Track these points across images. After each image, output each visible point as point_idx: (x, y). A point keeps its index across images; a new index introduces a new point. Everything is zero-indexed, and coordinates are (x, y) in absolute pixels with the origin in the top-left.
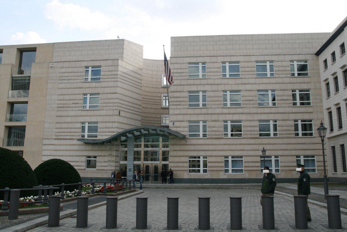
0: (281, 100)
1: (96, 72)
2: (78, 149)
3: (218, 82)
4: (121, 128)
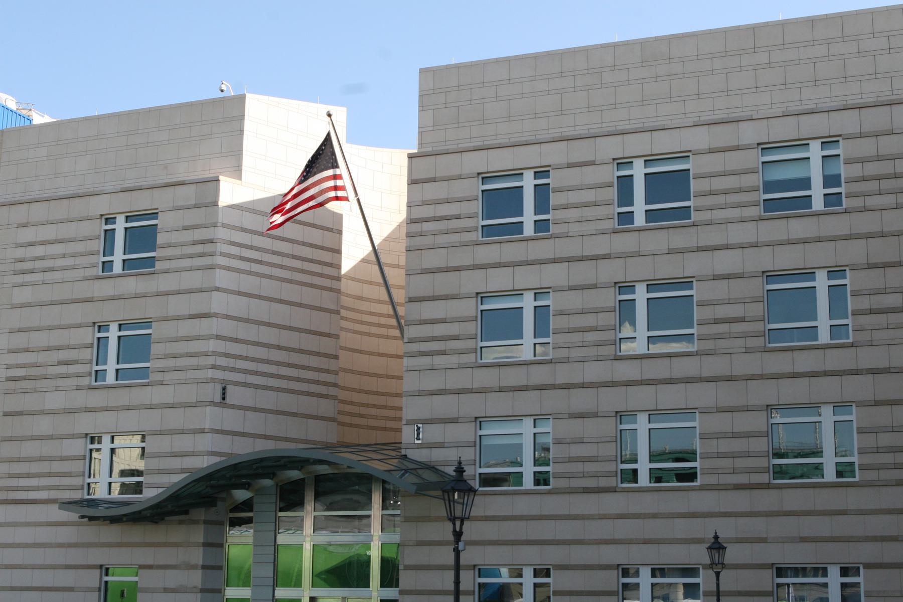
0: (872, 312)
1: (142, 237)
2: (74, 540)
3: (601, 246)
4: (213, 453)
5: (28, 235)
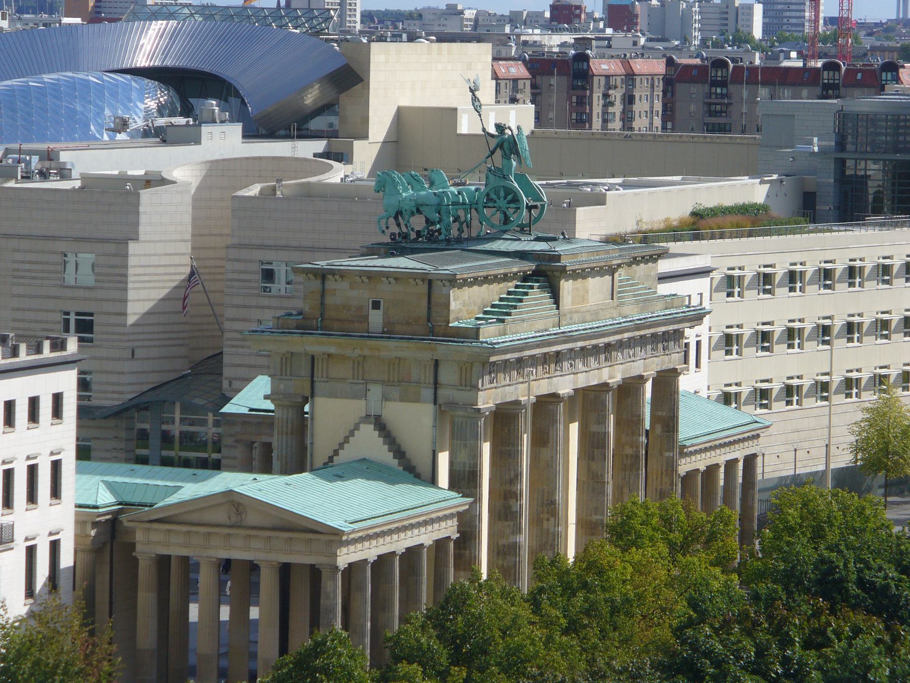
5: (19, 256)
